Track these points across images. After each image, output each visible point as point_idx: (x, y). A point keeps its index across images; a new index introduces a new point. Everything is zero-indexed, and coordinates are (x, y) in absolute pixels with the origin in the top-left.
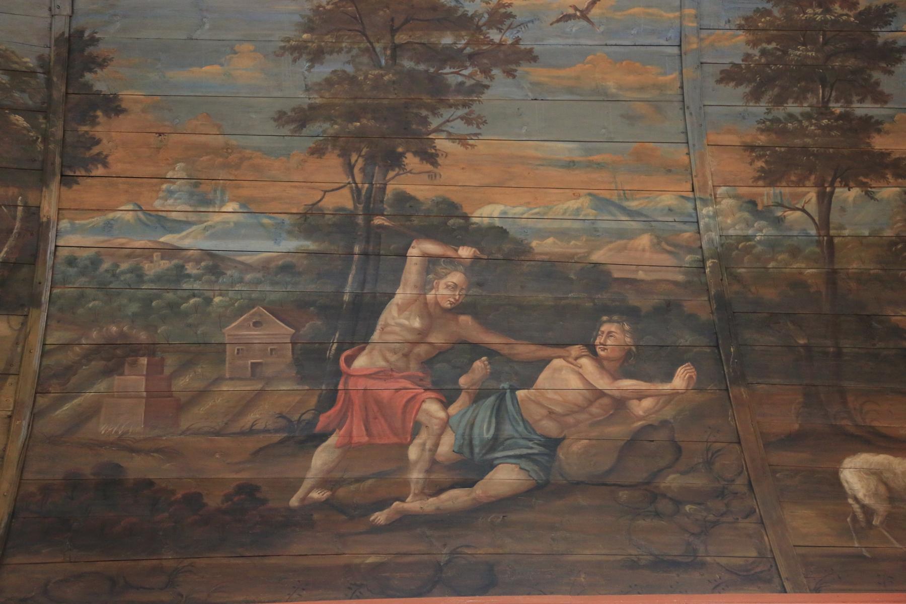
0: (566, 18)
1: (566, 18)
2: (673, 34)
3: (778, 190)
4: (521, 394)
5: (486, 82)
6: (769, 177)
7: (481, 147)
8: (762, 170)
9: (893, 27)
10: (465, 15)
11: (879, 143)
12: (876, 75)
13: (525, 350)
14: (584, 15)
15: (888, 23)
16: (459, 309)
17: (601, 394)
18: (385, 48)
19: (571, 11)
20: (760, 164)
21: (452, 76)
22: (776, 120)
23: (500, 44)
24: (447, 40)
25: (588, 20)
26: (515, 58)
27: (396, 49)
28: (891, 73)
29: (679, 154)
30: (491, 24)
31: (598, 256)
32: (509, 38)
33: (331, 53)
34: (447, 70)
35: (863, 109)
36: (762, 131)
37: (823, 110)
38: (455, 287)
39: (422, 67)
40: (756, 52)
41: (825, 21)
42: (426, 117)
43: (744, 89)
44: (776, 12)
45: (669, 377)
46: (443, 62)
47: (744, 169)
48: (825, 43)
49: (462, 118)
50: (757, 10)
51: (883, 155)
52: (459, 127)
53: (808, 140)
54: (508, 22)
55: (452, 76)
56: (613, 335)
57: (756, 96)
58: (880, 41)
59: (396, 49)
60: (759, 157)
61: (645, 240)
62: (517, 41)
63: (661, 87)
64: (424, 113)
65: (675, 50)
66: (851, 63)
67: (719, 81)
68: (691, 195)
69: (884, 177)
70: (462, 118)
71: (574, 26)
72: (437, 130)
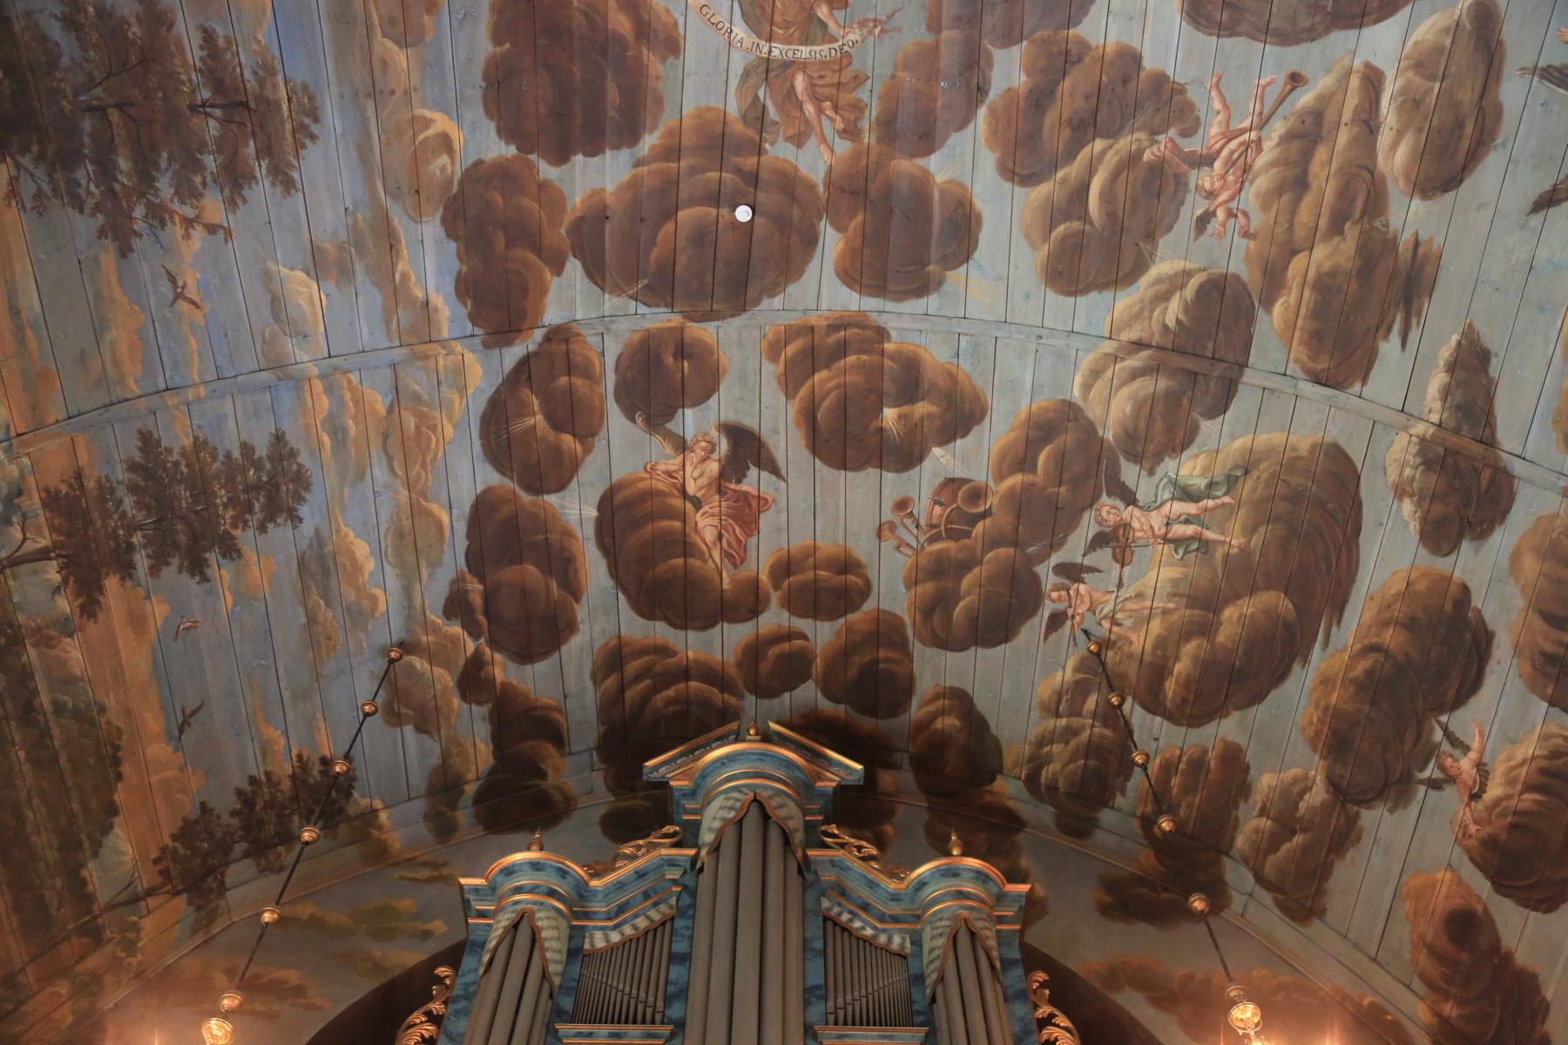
0: (173, 280)
1: (173, 280)
2: (178, 381)
3: (40, 512)
5: (87, 210)
6: (52, 501)
7: (12, 214)
8: (58, 492)
9: (221, 561)
10: (154, 179)
11: (111, 583)
12: (175, 561)
14: (178, 296)
15: (224, 557)
18: (98, 99)
19: (180, 283)
20: (64, 489)
21: (84, 174)
22: (112, 491)
23: (131, 219)
24: (124, 164)
25: (175, 300)
26: (120, 236)
27: (100, 111)
28: (180, 571)
29: (55, 412)
30: (150, 207)
32: (139, 226)
33: (79, 39)
34: (90, 168)
35: (141, 561)
36: (99, 481)
37: (132, 528)
39: (87, 140)
40: (176, 457)
41: (216, 507)
42: (30, 151)
43: (138, 456)
44: (216, 466)
46: (97, 162)
47: (56, 472)
48: (196, 512)
49: (39, 189)
50: (215, 449)
51: (101, 590)
52: (27, 188)
53: (99, 523)
54: (156, 223)
55: (84, 174)
57: (133, 467)
58: (207, 555)
59: (100, 111)
60: (70, 486)
62: (138, 235)
63: (122, 380)
64: (35, 148)
65: (162, 386)
66: (182, 539)
67: (139, 432)
68: (13, 434)
69: (78, 596)
70: (39, 189)
71: (166, 289)
72: (18, 165)
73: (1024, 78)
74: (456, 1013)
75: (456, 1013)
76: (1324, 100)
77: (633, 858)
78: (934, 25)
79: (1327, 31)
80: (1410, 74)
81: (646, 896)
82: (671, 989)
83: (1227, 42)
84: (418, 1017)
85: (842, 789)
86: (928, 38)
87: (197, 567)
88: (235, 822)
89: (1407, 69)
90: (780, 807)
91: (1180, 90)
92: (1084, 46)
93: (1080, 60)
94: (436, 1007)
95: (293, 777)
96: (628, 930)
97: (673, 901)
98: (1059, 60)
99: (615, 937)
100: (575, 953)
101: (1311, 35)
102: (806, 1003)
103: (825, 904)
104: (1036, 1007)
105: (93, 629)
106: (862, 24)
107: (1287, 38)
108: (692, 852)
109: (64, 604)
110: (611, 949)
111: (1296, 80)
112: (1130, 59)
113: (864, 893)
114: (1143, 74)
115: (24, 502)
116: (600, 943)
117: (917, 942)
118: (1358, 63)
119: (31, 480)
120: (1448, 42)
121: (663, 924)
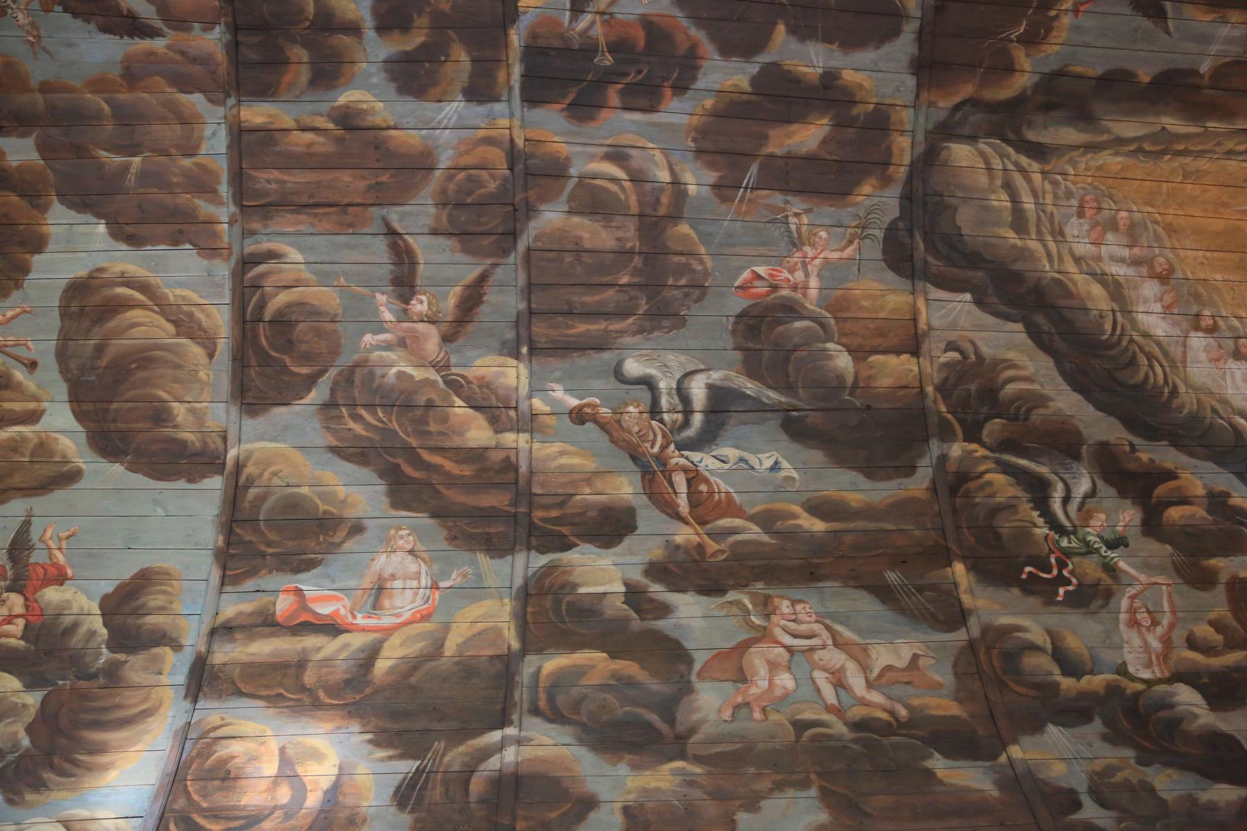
73: (15, 164)
76: (18, 388)
78: (45, 88)
79: (67, 380)
80: (36, 440)
83: (56, 313)
86: (34, 83)
89: (40, 438)
91: (18, 286)
92: (44, 209)
93: (33, 206)
98: (30, 190)
101: (64, 371)
106: (33, 25)
107: (62, 355)
111: (32, 365)
112: (38, 244)
114: (28, 256)
118: (45, 404)
120: (57, 459)
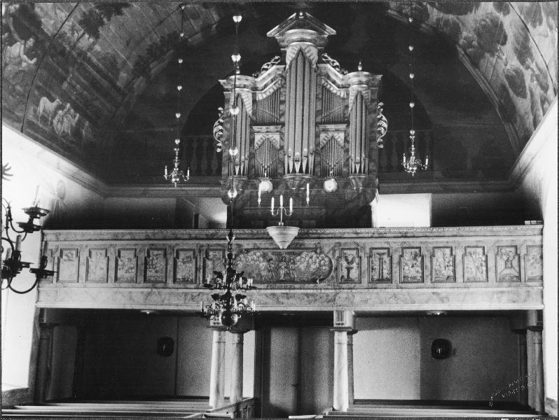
4: (9, 47)
6: (81, 23)
11: (100, 29)
13: (16, 36)
16: (12, 15)
17: (19, 56)
31: (43, 20)
35: (105, 20)
38: (15, 8)
45: (31, 60)
56: (31, 42)
61: (52, 22)
74: (226, 122)
75: (226, 122)
77: (267, 70)
81: (272, 81)
82: (281, 112)
84: (216, 123)
85: (330, 37)
87: (120, 13)
88: (149, 55)
90: (308, 52)
94: (221, 121)
95: (161, 41)
96: (268, 94)
97: (280, 82)
99: (265, 96)
100: (254, 101)
102: (316, 116)
103: (323, 82)
104: (379, 114)
105: (100, 40)
108: (284, 66)
109: (92, 40)
110: (264, 100)
113: (333, 77)
115: (76, 28)
116: (261, 98)
117: (348, 94)
119: (75, 22)
121: (277, 90)
